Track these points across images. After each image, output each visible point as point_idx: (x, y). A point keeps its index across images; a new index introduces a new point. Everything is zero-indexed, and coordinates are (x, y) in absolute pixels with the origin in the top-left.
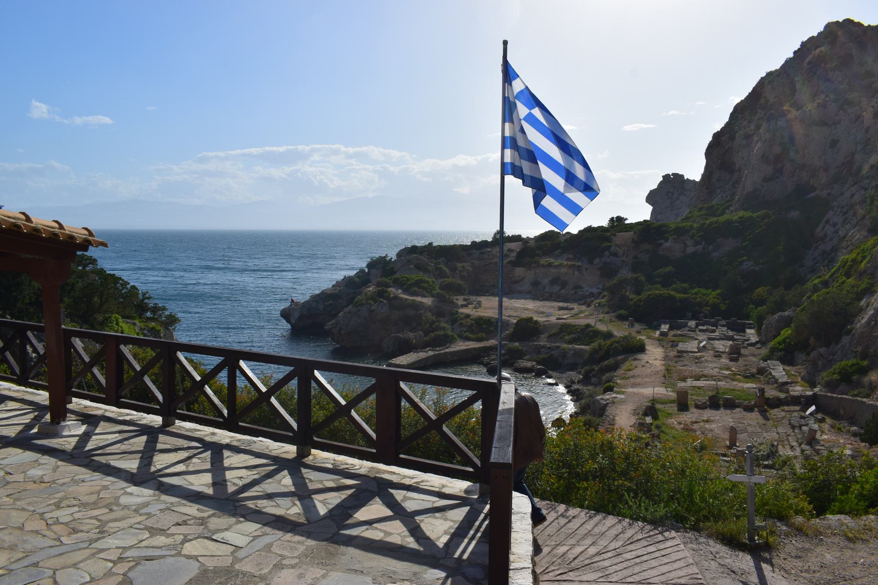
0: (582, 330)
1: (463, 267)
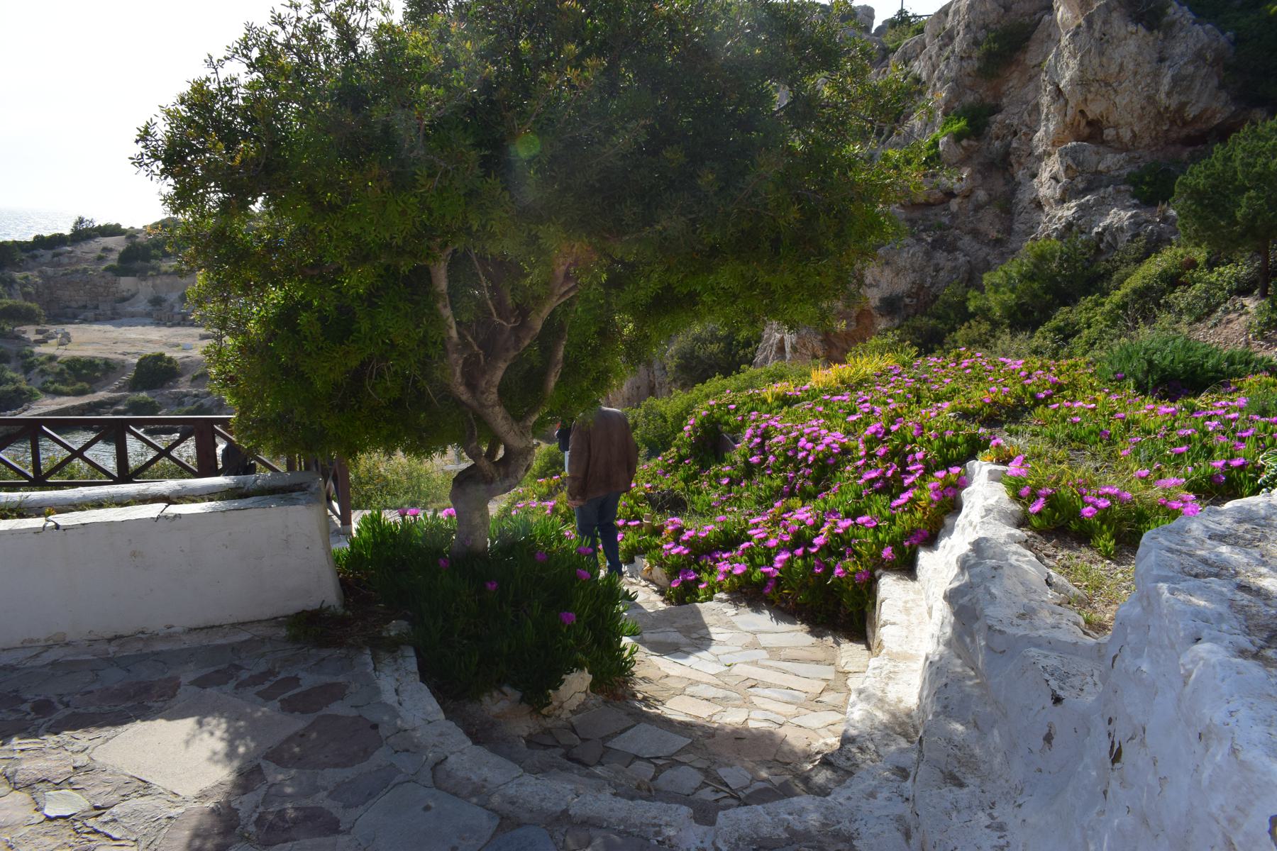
1: (26, 278)
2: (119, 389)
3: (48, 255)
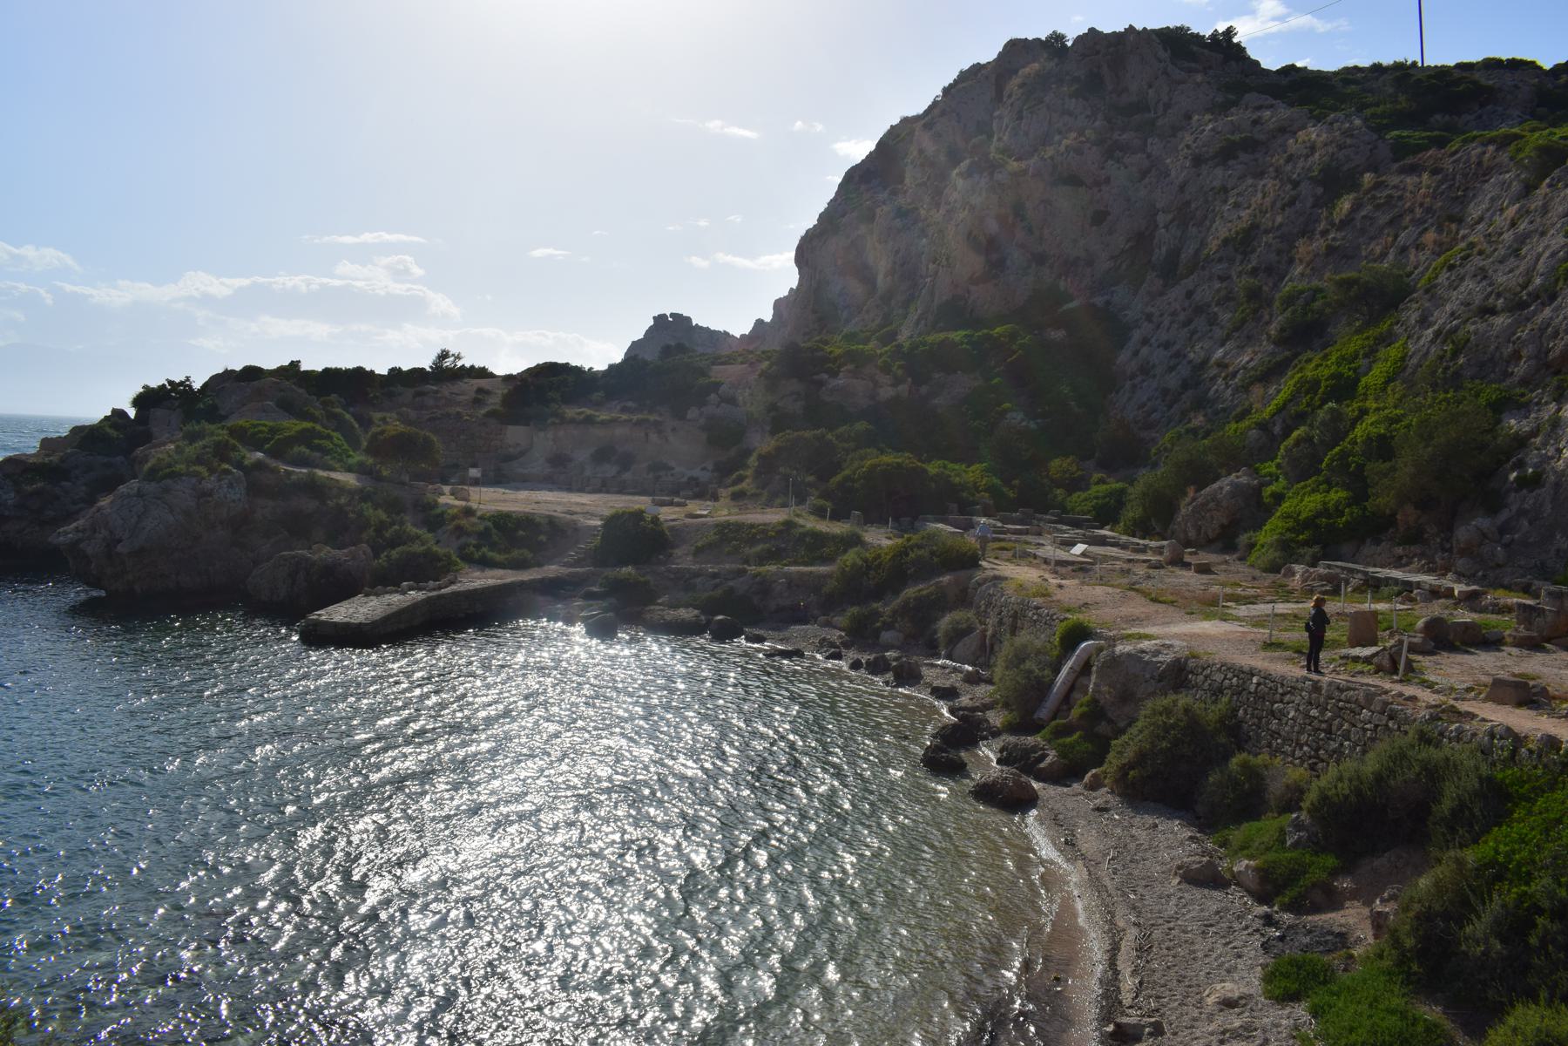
0: (779, 532)
2: (578, 563)
3: (409, 392)
